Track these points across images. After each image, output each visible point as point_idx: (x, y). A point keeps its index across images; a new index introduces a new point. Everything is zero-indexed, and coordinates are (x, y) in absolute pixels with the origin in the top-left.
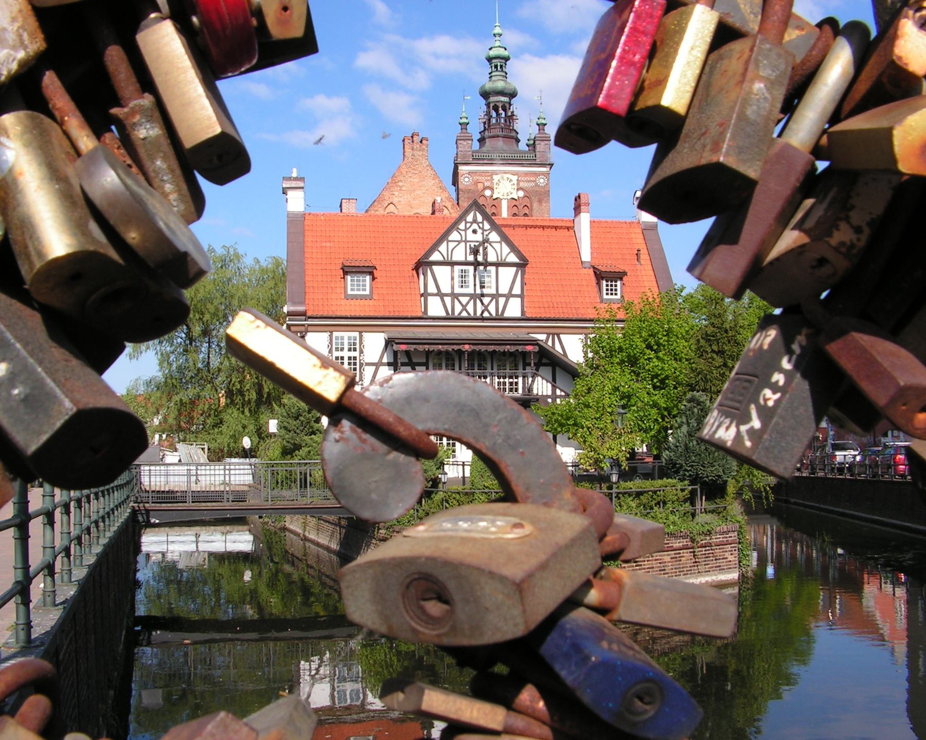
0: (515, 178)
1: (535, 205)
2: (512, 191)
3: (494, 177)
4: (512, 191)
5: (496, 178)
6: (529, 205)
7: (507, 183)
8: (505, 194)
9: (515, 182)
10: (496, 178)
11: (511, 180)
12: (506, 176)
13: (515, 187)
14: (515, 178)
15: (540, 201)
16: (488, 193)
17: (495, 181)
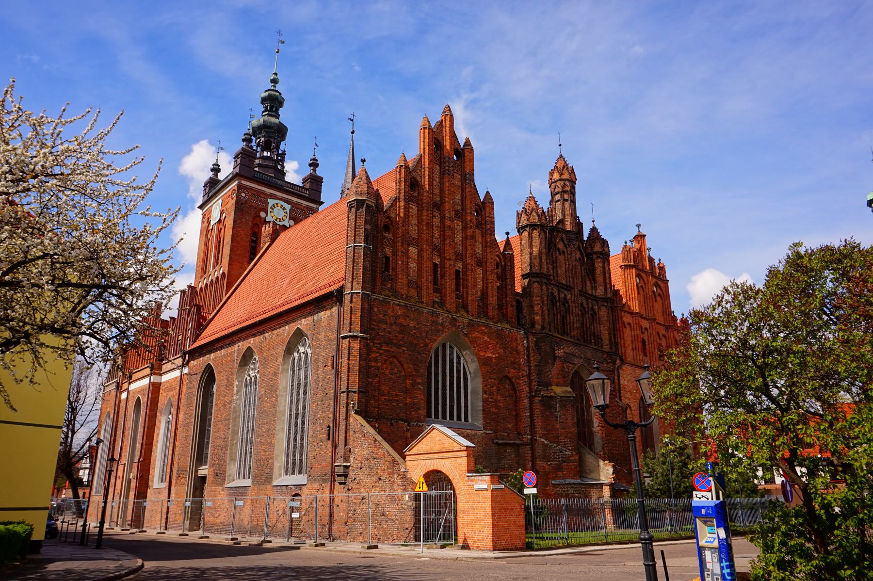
2: (284, 218)
3: (269, 200)
4: (284, 218)
5: (271, 202)
7: (282, 212)
10: (271, 202)
11: (284, 209)
13: (288, 215)
16: (263, 214)
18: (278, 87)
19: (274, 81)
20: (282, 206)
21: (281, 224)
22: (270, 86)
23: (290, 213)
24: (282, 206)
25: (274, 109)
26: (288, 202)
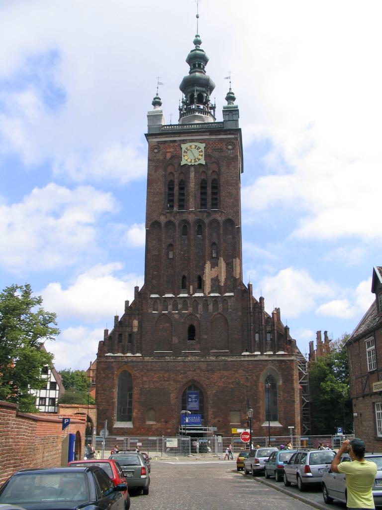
0: (202, 146)
1: (223, 169)
2: (200, 157)
4: (200, 157)
5: (184, 146)
6: (217, 170)
7: (196, 153)
8: (193, 161)
9: (203, 149)
10: (184, 146)
11: (199, 148)
12: (193, 145)
13: (203, 153)
14: (202, 146)
15: (228, 165)
17: (184, 149)
18: (201, 47)
19: (197, 42)
20: (196, 146)
21: (196, 164)
22: (193, 47)
23: (205, 152)
24: (196, 146)
25: (197, 66)
26: (201, 141)
